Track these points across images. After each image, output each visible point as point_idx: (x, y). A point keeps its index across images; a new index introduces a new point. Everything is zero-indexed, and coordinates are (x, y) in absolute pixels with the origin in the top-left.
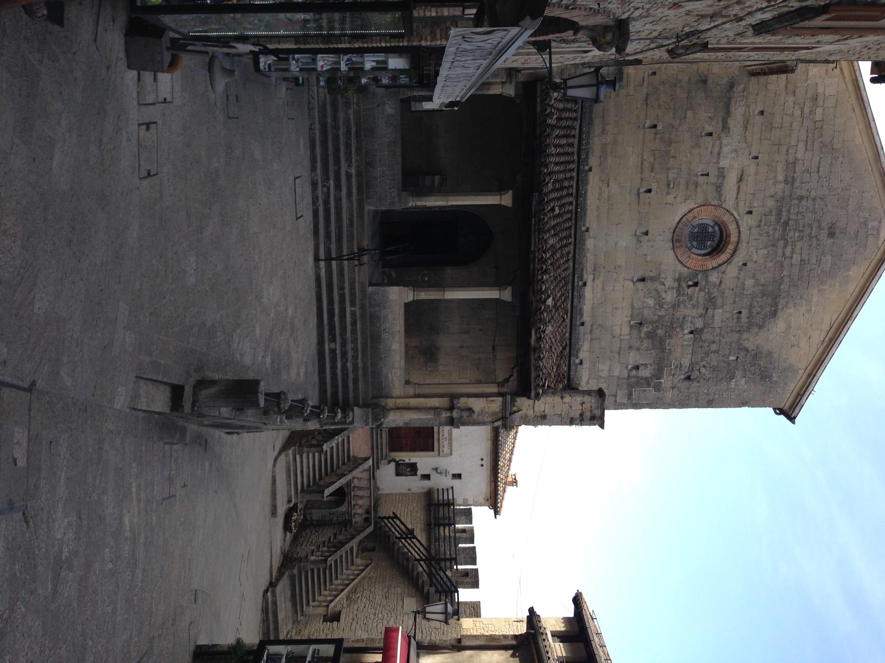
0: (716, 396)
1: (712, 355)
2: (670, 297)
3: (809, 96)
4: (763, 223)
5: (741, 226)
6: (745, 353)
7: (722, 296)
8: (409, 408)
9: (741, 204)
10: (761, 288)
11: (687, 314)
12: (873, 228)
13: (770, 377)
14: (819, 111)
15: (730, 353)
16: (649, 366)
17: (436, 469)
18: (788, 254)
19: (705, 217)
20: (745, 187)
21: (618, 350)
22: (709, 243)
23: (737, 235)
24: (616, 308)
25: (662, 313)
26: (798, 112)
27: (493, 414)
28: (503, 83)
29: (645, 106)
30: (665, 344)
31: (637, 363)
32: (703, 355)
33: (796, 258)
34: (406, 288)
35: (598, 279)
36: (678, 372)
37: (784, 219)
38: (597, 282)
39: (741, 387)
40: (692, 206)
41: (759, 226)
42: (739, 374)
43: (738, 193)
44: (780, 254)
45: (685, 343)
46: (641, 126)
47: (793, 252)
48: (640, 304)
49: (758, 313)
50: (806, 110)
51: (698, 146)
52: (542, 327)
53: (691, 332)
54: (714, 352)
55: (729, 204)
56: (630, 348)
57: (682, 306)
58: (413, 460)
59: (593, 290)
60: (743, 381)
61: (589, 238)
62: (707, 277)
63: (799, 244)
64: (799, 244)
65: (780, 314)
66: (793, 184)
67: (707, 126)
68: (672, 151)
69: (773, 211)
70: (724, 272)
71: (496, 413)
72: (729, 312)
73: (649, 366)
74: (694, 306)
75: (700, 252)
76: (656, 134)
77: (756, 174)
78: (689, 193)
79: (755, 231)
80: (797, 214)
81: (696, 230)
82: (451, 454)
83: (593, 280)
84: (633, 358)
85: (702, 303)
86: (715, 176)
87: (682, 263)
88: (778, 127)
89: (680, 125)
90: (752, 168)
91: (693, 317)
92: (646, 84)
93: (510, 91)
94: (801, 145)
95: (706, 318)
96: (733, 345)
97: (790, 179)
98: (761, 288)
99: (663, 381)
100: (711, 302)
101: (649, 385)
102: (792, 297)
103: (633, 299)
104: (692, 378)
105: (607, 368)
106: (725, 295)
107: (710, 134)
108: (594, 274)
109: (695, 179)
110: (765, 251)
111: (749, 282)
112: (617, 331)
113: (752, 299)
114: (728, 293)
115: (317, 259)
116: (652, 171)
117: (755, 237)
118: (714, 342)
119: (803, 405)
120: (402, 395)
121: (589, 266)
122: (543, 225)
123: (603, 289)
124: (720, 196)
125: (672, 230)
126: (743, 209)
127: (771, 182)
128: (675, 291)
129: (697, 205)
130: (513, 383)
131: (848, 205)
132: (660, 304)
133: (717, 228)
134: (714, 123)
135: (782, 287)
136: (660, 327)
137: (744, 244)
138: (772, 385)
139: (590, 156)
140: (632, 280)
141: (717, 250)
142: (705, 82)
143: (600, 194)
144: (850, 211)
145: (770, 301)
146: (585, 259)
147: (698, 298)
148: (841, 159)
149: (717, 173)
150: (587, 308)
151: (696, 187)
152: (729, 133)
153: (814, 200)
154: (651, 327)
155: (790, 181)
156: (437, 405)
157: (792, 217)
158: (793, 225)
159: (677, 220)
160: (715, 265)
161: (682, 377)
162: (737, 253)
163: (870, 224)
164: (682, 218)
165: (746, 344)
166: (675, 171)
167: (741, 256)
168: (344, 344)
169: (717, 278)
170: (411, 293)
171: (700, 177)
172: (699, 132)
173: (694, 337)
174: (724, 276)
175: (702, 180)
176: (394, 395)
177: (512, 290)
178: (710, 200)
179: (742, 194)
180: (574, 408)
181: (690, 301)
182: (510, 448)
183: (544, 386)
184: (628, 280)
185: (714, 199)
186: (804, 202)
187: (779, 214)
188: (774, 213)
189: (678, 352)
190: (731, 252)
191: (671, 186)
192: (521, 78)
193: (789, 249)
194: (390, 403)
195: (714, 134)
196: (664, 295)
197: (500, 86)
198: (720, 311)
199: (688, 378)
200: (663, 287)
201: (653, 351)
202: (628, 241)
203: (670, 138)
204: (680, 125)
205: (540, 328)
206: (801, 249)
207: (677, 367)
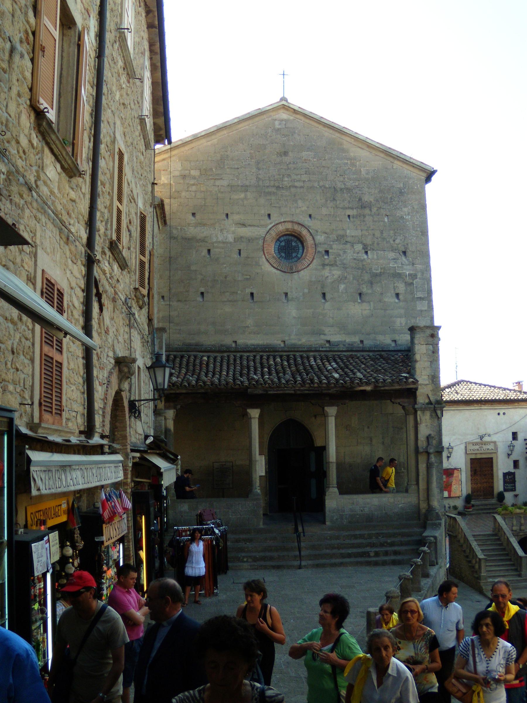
0: (418, 229)
2: (337, 273)
3: (182, 181)
4: (277, 205)
5: (280, 221)
8: (428, 490)
9: (262, 222)
10: (329, 201)
12: (280, 124)
14: (193, 173)
16: (395, 285)
17: (509, 455)
18: (301, 184)
19: (272, 248)
21: (383, 311)
22: (294, 244)
23: (286, 224)
24: (348, 314)
26: (194, 188)
28: (165, 419)
31: (394, 295)
32: (385, 242)
33: (305, 177)
34: (327, 493)
37: (274, 190)
38: (326, 332)
39: (410, 211)
40: (264, 259)
41: (280, 207)
42: (399, 213)
44: (302, 190)
45: (375, 257)
50: (192, 182)
51: (217, 260)
52: (357, 381)
53: (366, 253)
54: (382, 233)
55: (262, 232)
56: (380, 301)
57: (345, 261)
58: (501, 476)
59: (332, 334)
60: (405, 210)
64: (294, 177)
66: (247, 186)
67: (203, 254)
71: (431, 416)
74: (345, 252)
75: (301, 251)
76: (208, 292)
77: (238, 213)
78: (254, 263)
81: (283, 255)
82: (495, 443)
83: (325, 335)
84: (390, 299)
87: (309, 264)
93: (170, 414)
94: (218, 183)
96: (376, 219)
98: (329, 201)
99: (407, 273)
100: (341, 239)
101: (412, 284)
104: (404, 250)
105: (398, 320)
107: (209, 251)
108: (320, 334)
110: (300, 203)
111: (324, 211)
112: (366, 312)
115: (300, 567)
116: (237, 293)
118: (374, 235)
120: (417, 495)
122: (273, 384)
123: (332, 326)
124: (257, 239)
125: (283, 274)
128: (332, 268)
129: (263, 256)
130: (405, 401)
131: (263, 144)
132: (342, 279)
133: (282, 239)
135: (327, 186)
140: (324, 303)
141: (299, 238)
144: (267, 142)
147: (337, 249)
148: (229, 153)
151: (249, 258)
153: (259, 169)
155: (245, 188)
156: (424, 465)
157: (272, 183)
160: (311, 238)
161: (404, 258)
163: (277, 126)
168: (372, 545)
169: (321, 236)
170: (331, 490)
171: (241, 256)
173: (370, 250)
174: (319, 231)
176: (417, 502)
177: (327, 406)
181: (340, 255)
182: (489, 388)
183: (406, 377)
187: (270, 193)
188: (269, 198)
191: (248, 277)
192: (161, 405)
193: (297, 184)
194: (423, 506)
195: (209, 248)
196: (336, 277)
197: (168, 421)
198: (348, 231)
199: (404, 253)
200: (329, 277)
204: (202, 275)
205: (358, 383)
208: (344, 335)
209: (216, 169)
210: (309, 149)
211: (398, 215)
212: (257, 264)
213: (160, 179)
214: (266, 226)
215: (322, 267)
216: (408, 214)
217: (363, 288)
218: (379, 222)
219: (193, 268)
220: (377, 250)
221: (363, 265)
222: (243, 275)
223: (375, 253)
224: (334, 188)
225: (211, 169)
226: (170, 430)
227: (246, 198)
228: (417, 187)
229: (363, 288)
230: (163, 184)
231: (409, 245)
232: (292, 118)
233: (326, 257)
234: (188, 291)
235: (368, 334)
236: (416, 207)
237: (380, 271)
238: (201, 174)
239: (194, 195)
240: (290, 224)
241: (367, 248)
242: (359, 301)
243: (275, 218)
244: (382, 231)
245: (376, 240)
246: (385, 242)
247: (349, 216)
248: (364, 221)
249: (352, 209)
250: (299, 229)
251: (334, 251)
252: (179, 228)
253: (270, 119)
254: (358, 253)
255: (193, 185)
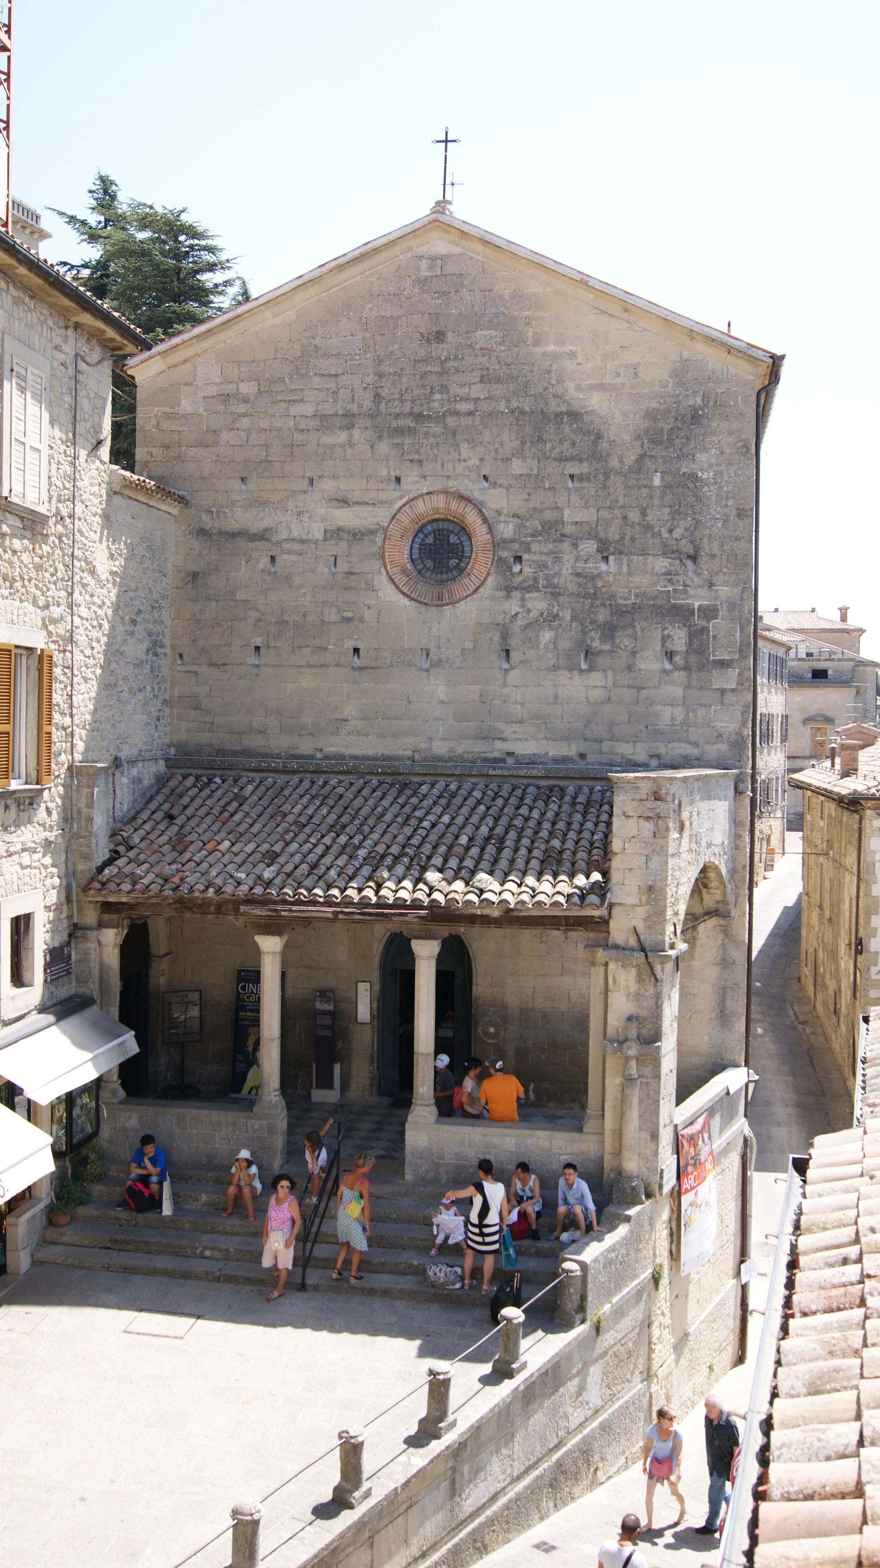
0: (730, 503)
1: (649, 518)
2: (538, 604)
3: (221, 408)
4: (416, 457)
5: (419, 492)
6: (647, 460)
7: (541, 511)
9: (383, 496)
10: (528, 444)
11: (570, 571)
12: (430, 268)
13: (695, 409)
15: (646, 487)
16: (666, 632)
18: (470, 406)
20: (356, 494)
21: (634, 691)
24: (556, 697)
25: (567, 615)
26: (245, 423)
27: (640, 980)
29: (227, 667)
30: (625, 606)
33: (478, 391)
35: (502, 732)
36: (680, 578)
37: (410, 423)
38: (507, 733)
39: (713, 461)
40: (384, 578)
43: (366, 503)
44: (469, 420)
45: (625, 569)
46: (255, 671)
47: (466, 399)
48: (550, 655)
49: (574, 444)
51: (288, 578)
53: (606, 559)
54: (644, 514)
55: (382, 516)
57: (556, 581)
59: (520, 740)
60: (702, 457)
61: (430, 749)
62: (504, 541)
63: (455, 390)
64: (455, 390)
65: (576, 407)
66: (354, 415)
67: (261, 566)
68: (296, 618)
69: (396, 441)
70: (499, 512)
71: (639, 974)
72: (569, 496)
73: (666, 632)
74: (557, 560)
77: (335, 477)
78: (363, 585)
79: (428, 468)
80: (402, 400)
85: (551, 546)
86: (337, 544)
88: (267, 451)
89: (257, 610)
90: (328, 486)
91: (577, 561)
92: (194, 668)
94: (295, 410)
95: (580, 535)
96: (632, 482)
97: (346, 422)
98: (528, 444)
99: (696, 604)
101: (704, 630)
102: (546, 388)
103: (540, 669)
104: (692, 552)
105: (668, 710)
106: (538, 506)
107: (273, 558)
108: (494, 739)
109: (340, 577)
110: (464, 448)
111: (517, 467)
112: (597, 694)
113: (547, 459)
114: (535, 502)
116: (326, 649)
117: (439, 467)
118: (625, 518)
119: (748, 344)
121: (479, 748)
123: (520, 722)
124: (372, 532)
125: (422, 609)
126: (390, 492)
127: (349, 451)
128: (527, 596)
129: (383, 571)
132: (550, 619)
134: (255, 554)
135: (527, 409)
136: (592, 616)
137: (451, 483)
138: (711, 404)
139: (298, 752)
140: (506, 671)
142: (195, 575)
143: (359, 733)
144: (401, 312)
145: (551, 428)
146: (466, 756)
148: (318, 341)
149: (333, 542)
150: (555, 750)
151: (353, 574)
152: (271, 528)
153: (381, 376)
154: (593, 634)
155: (349, 420)
157: (407, 410)
158: (422, 405)
159: (405, 601)
160: (485, 529)
162: (467, 493)
163: (425, 273)
164: (404, 594)
165: (631, 458)
166: (326, 611)
167: (470, 486)
169: (508, 523)
172: (268, 578)
173: (613, 554)
174: (505, 512)
175: (343, 566)
178: (374, 549)
179: (366, 497)
180: (634, 832)
181: (546, 567)
184: (505, 678)
185: (373, 542)
186: (384, 392)
187: (399, 431)
188: (398, 440)
189: (641, 581)
190: (463, 504)
191: (350, 615)
193: (463, 407)
195: (273, 553)
196: (534, 614)
198: (567, 512)
199: (694, 558)
200: (520, 616)
201: (638, 628)
202: (437, 682)
203: (276, 623)
204: (257, 610)
206: (462, 386)
207: (670, 581)
208: (544, 742)
209: (291, 378)
210: (491, 325)
211: (683, 470)
212: (370, 587)
213: (179, 405)
214: (389, 503)
215: (504, 593)
216: (710, 466)
217: (592, 639)
218: (639, 488)
219: (240, 595)
220: (631, 553)
221: (595, 588)
222: (339, 610)
223: (625, 559)
224: (542, 412)
225: (282, 379)
226: (109, 968)
227: (351, 444)
228: (736, 402)
229: (592, 639)
230: (184, 416)
231: (706, 540)
232: (456, 250)
233: (517, 568)
234: (228, 644)
235: (598, 741)
236: (728, 451)
237: (633, 600)
238: (260, 392)
239: (245, 438)
240: (442, 497)
241: (607, 549)
242: (584, 667)
243: (413, 483)
244: (645, 509)
245: (629, 531)
246: (649, 535)
247: (572, 477)
248: (605, 487)
249: (581, 461)
250: (460, 510)
251: (533, 557)
252: (214, 510)
253: (409, 255)
254: (586, 561)
255: (244, 415)
